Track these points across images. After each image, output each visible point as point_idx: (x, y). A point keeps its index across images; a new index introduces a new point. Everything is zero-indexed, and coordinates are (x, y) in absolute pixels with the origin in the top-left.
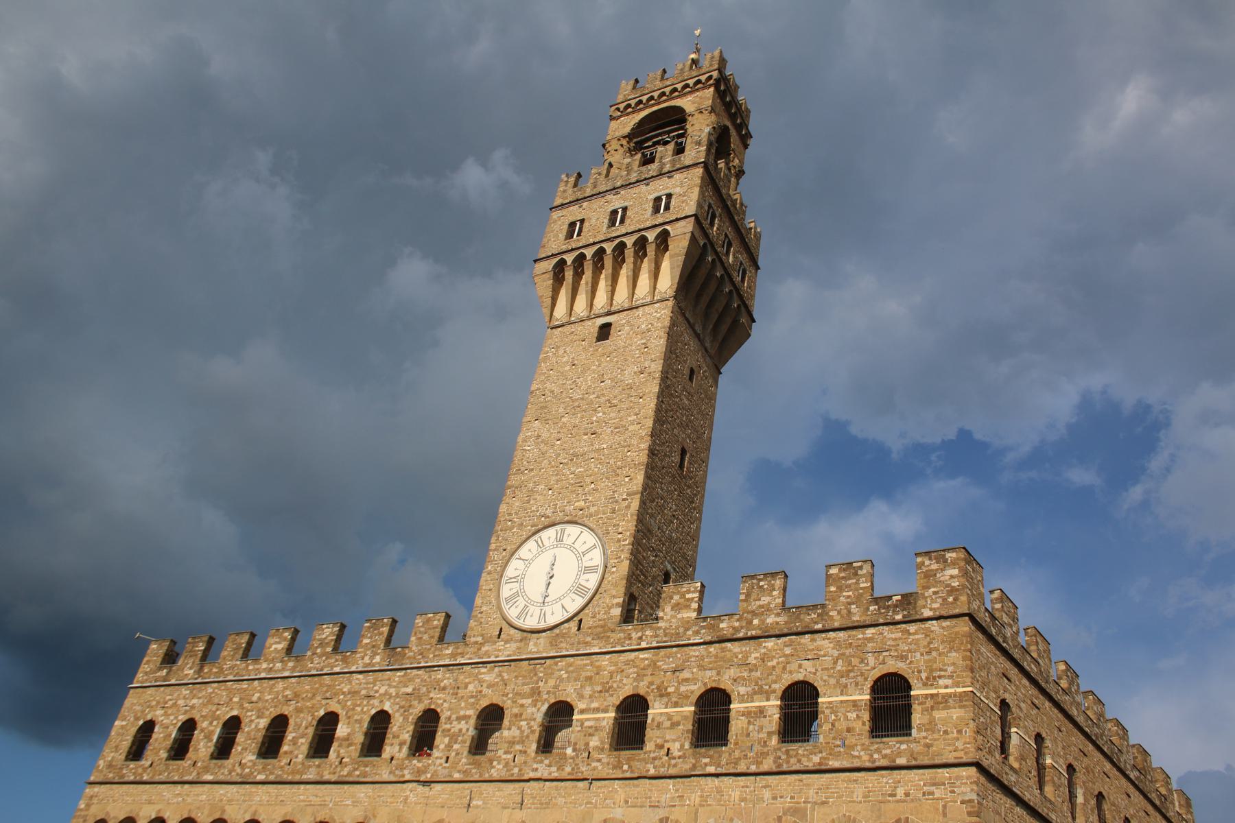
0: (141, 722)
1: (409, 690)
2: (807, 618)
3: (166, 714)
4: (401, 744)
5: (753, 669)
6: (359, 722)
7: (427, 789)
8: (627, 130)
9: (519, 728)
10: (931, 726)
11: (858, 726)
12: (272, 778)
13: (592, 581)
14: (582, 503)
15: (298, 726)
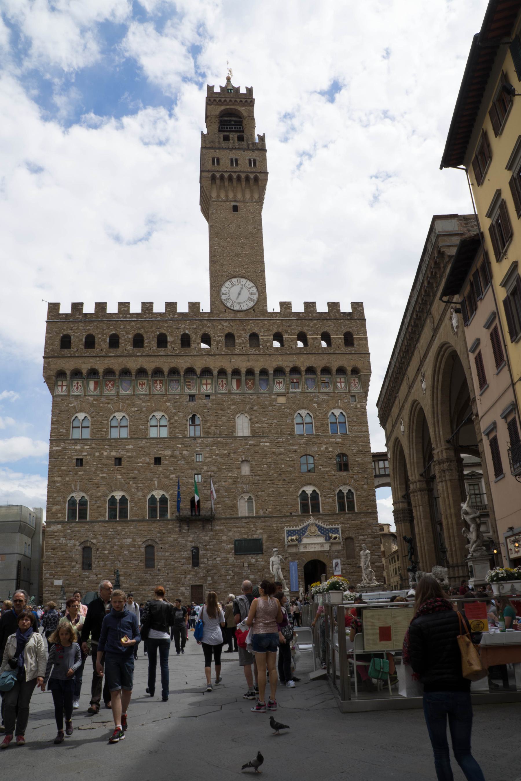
0: (61, 335)
1: (195, 327)
2: (325, 315)
3: (74, 332)
4: (199, 344)
5: (312, 327)
6: (177, 336)
7: (213, 357)
8: (217, 113)
9: (242, 340)
10: (359, 345)
11: (342, 344)
12: (144, 354)
13: (255, 297)
14: (244, 271)
15: (148, 338)
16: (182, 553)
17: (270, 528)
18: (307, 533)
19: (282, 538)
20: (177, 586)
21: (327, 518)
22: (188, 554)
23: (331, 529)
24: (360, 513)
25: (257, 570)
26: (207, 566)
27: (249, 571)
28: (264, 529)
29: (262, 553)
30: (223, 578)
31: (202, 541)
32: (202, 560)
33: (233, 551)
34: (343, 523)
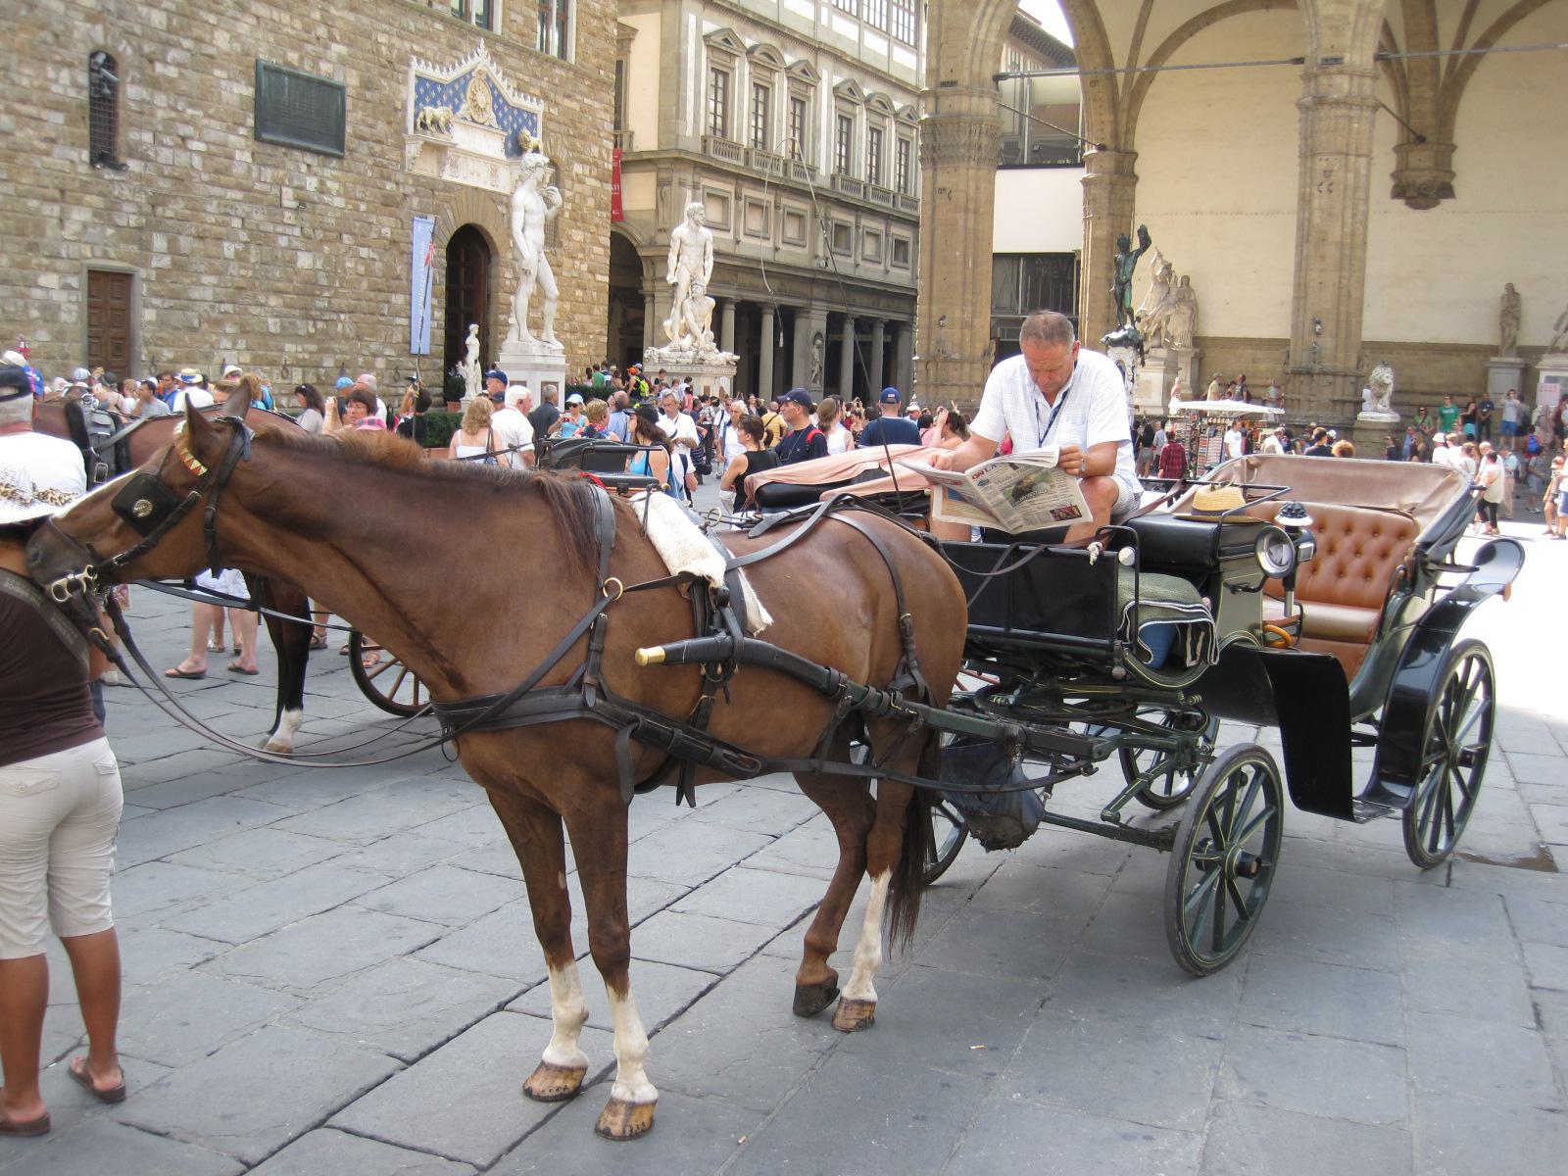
16: (51, 74)
17: (368, 45)
18: (464, 106)
19: (399, 105)
20: (23, 266)
21: (512, 62)
22: (75, 85)
23: (521, 111)
24: (584, 76)
25: (320, 234)
26: (151, 171)
27: (297, 232)
28: (350, 45)
29: (340, 158)
30: (212, 249)
31: (137, 29)
32: (134, 135)
33: (251, 122)
34: (546, 98)
